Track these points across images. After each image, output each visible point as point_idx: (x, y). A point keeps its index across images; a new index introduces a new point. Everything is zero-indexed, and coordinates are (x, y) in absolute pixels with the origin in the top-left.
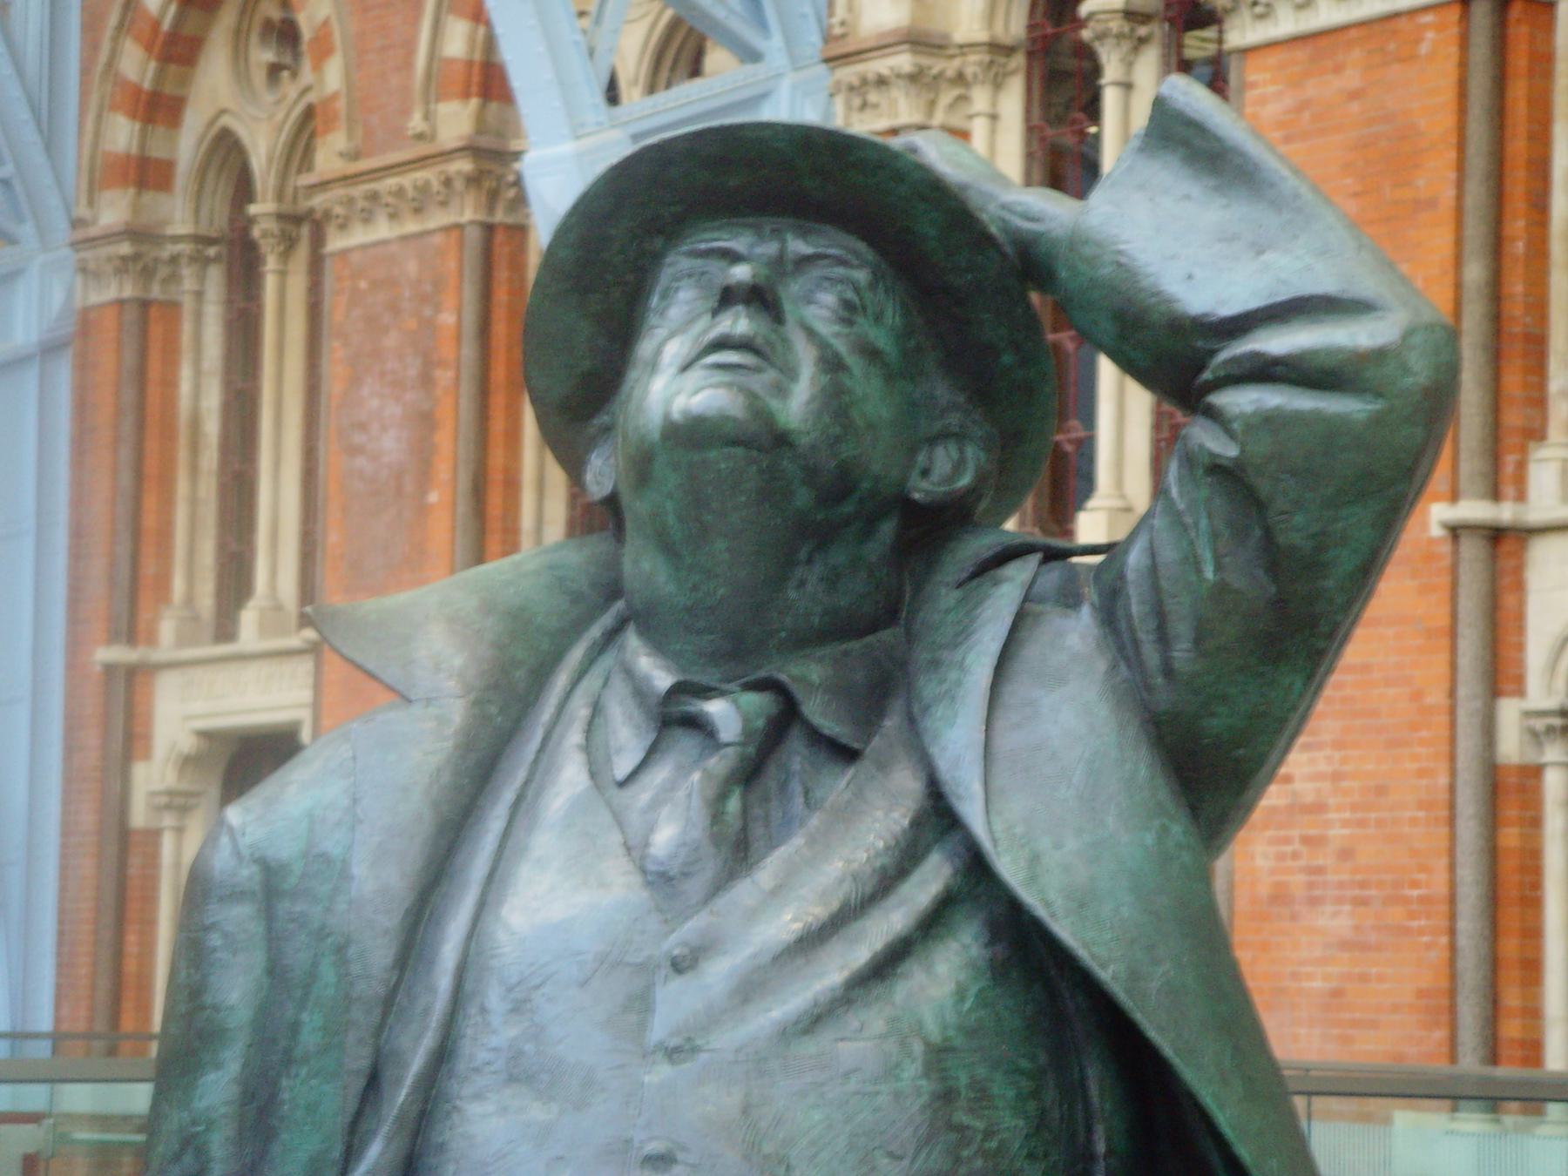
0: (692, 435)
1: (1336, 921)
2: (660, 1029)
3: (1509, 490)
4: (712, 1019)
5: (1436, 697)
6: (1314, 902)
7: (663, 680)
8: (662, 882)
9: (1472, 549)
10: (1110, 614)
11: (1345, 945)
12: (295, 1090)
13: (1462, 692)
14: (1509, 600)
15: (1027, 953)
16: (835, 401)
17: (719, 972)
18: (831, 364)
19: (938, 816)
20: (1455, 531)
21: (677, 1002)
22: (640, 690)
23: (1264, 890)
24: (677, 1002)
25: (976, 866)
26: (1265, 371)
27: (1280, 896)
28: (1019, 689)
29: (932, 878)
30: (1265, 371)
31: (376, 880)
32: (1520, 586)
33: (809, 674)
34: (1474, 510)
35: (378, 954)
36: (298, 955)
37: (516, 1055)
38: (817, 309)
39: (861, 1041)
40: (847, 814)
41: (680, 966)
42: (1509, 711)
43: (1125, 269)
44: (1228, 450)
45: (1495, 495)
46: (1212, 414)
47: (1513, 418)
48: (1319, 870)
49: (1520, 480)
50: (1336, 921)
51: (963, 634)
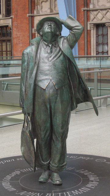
0: (47, 32)
1: (21, 45)
2: (50, 60)
3: (33, 13)
4: (52, 60)
5: (28, 28)
6: (19, 44)
7: (47, 44)
8: (49, 53)
9: (30, 17)
10: (67, 40)
11: (22, 47)
12: (30, 64)
13: (30, 28)
14: (33, 21)
15: (65, 56)
16: (54, 30)
17: (52, 57)
18: (54, 28)
19: (60, 49)
20: (29, 16)
21: (50, 59)
22: (45, 44)
23: (15, 43)
24: (50, 59)
25: (62, 51)
26: (75, 29)
27: (17, 44)
28: (63, 44)
29: (60, 53)
30: (75, 29)
31: (33, 53)
32: (34, 20)
33: (53, 43)
34: (30, 15)
35: (35, 57)
36: (30, 57)
37: (43, 61)
38: (52, 26)
39: (58, 60)
40: (56, 50)
41: (50, 57)
42: (33, 29)
43: (68, 24)
44: (73, 32)
45: (32, 13)
46: (73, 31)
47: (33, 8)
48: (19, 42)
49: (34, 12)
50: (21, 45)
51: (60, 41)
